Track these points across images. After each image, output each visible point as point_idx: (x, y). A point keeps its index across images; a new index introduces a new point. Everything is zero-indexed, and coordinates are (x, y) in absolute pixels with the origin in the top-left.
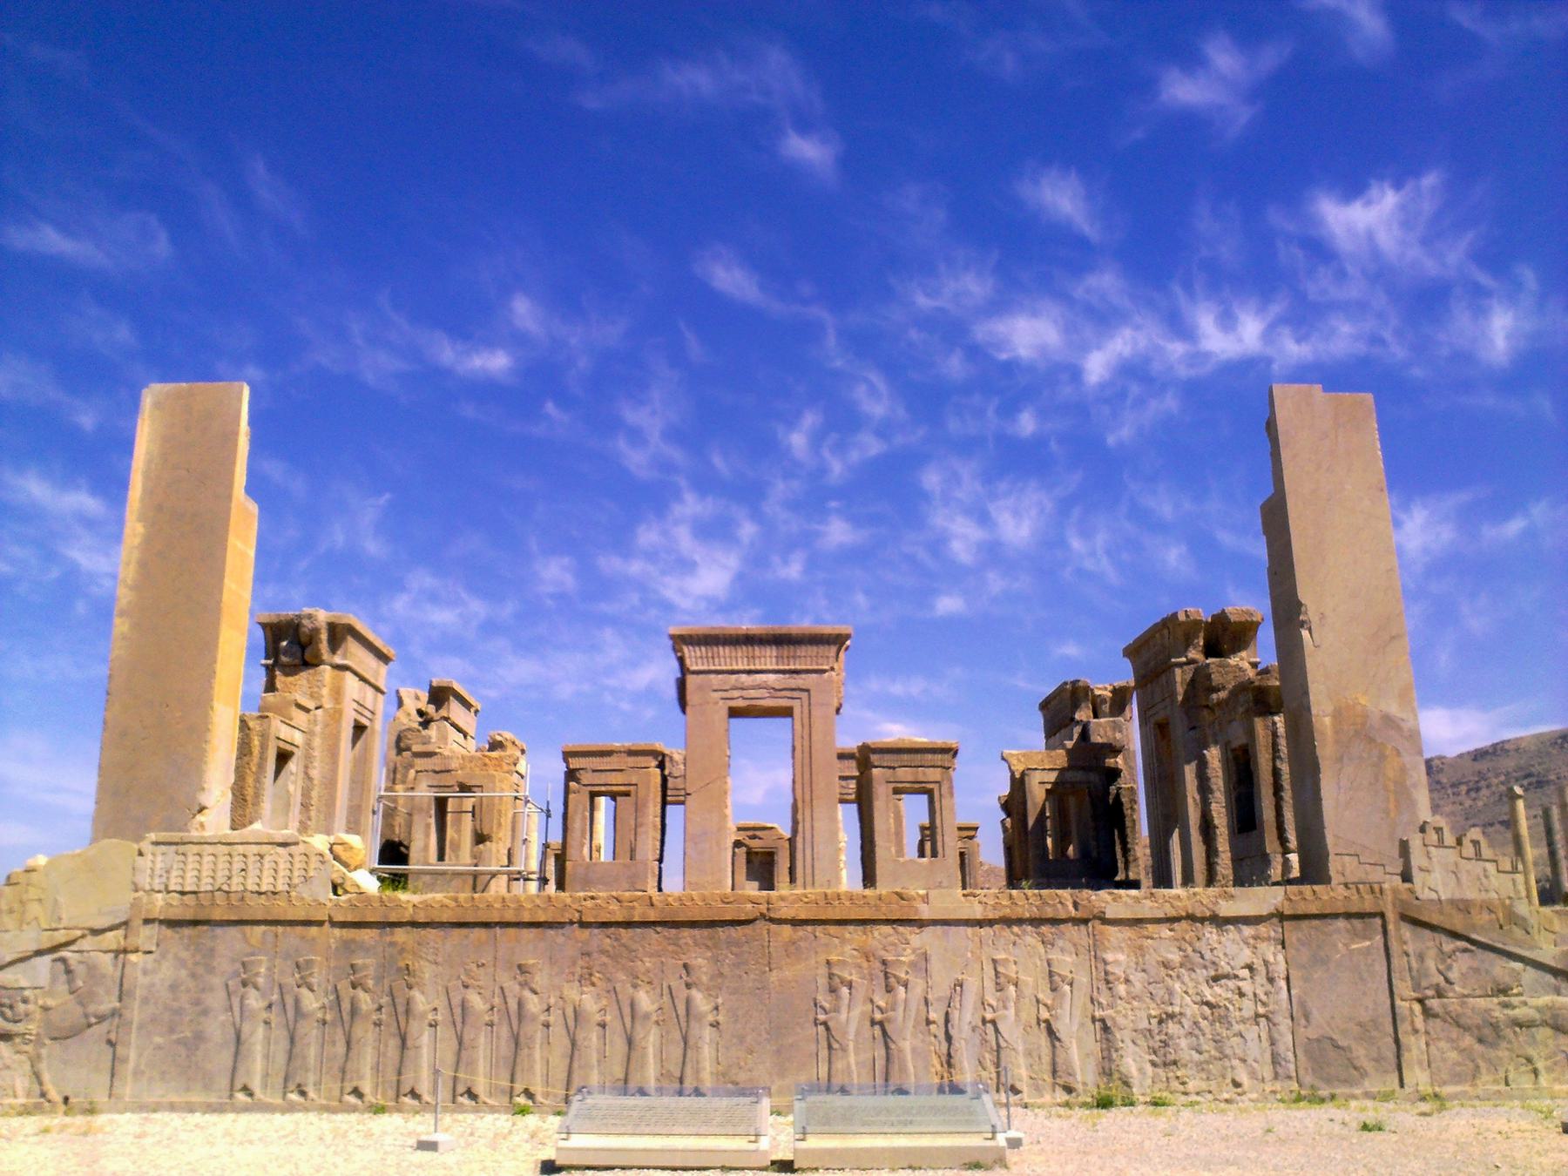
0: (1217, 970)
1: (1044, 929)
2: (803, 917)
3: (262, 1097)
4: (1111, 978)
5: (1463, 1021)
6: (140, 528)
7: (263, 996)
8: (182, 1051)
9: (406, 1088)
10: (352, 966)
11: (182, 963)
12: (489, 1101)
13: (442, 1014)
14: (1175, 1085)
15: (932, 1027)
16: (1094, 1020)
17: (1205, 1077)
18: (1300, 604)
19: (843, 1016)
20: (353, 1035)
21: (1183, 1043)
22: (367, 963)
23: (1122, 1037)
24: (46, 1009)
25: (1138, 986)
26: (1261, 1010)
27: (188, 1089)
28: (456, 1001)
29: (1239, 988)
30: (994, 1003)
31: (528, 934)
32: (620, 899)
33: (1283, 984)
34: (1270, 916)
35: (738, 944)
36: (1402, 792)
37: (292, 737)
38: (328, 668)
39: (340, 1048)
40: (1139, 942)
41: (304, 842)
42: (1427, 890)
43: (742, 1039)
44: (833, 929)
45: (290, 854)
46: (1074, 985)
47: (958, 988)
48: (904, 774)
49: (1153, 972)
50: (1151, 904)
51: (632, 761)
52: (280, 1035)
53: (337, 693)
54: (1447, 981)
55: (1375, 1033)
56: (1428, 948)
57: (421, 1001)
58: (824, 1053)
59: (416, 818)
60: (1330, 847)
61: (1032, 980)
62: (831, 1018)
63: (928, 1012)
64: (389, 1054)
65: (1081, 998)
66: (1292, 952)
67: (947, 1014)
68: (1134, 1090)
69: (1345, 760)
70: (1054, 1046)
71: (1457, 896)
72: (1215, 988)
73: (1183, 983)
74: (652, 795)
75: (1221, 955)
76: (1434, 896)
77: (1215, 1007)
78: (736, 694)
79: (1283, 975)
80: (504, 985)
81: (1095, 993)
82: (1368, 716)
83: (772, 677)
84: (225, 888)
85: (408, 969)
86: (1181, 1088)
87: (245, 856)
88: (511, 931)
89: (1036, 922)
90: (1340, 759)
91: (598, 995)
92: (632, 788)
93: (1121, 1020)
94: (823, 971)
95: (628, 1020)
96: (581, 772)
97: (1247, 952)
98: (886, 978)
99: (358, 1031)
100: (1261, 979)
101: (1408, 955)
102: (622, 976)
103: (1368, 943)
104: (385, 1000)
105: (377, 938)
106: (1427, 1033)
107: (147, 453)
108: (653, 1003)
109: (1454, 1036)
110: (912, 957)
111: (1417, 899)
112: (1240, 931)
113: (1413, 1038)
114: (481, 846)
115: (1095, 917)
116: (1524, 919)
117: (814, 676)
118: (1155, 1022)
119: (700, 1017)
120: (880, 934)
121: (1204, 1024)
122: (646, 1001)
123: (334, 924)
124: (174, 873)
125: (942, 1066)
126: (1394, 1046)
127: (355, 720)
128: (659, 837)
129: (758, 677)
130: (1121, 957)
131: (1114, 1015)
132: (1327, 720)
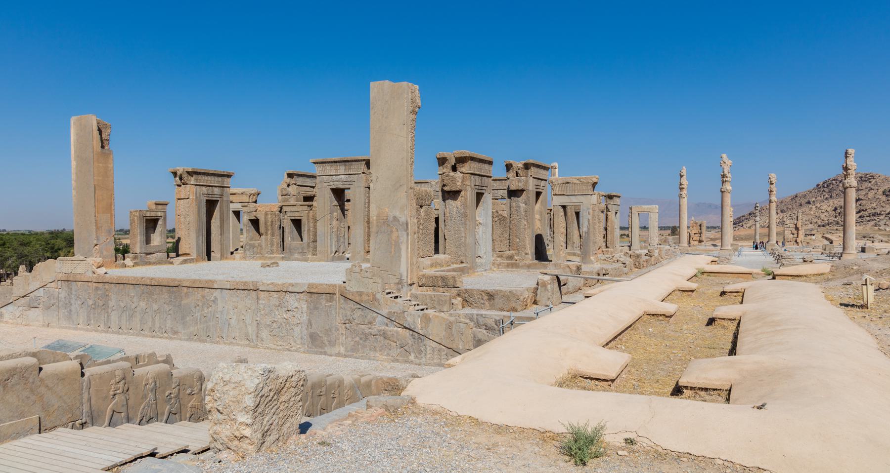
15: (217, 319)
19: (196, 315)
24: (43, 302)
26: (298, 322)
36: (397, 245)
55: (330, 333)
69: (379, 233)
76: (351, 289)
78: (332, 183)
82: (388, 217)
90: (377, 233)
97: (296, 304)
103: (330, 304)
106: (345, 334)
116: (378, 300)
117: (357, 175)
121: (284, 324)
132: (375, 218)
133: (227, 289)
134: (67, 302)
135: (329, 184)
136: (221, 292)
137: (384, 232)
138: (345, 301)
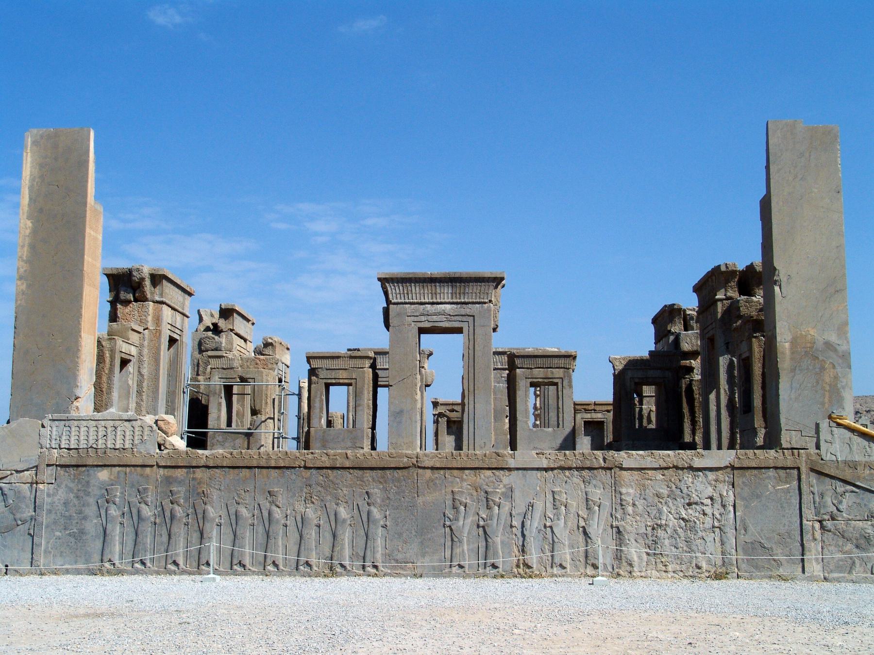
0: (690, 500)
1: (585, 473)
2: (438, 465)
3: (120, 566)
4: (624, 503)
5: (846, 535)
6: (29, 224)
7: (119, 508)
8: (73, 540)
10: (171, 491)
11: (71, 490)
12: (251, 568)
13: (224, 519)
14: (660, 566)
15: (514, 529)
16: (612, 527)
17: (679, 563)
18: (775, 269)
19: (461, 523)
20: (172, 531)
21: (667, 542)
22: (180, 491)
23: (630, 538)
25: (640, 507)
26: (716, 524)
27: (76, 562)
28: (232, 511)
29: (703, 511)
30: (552, 517)
31: (274, 473)
32: (328, 454)
33: (731, 509)
34: (726, 467)
35: (399, 480)
37: (130, 352)
38: (151, 303)
39: (165, 538)
40: (643, 482)
41: (141, 419)
42: (829, 454)
43: (400, 535)
44: (455, 472)
45: (132, 427)
46: (601, 507)
47: (530, 508)
48: (539, 373)
49: (650, 500)
50: (652, 459)
51: (352, 363)
52: (130, 530)
54: (838, 510)
56: (827, 490)
57: (211, 511)
58: (448, 543)
59: (211, 399)
60: (782, 425)
61: (576, 504)
62: (453, 524)
63: (512, 521)
64: (193, 542)
65: (606, 512)
66: (738, 490)
67: (523, 523)
68: (635, 569)
69: (798, 371)
70: (587, 542)
71: (849, 458)
72: (689, 510)
73: (668, 506)
74: (366, 386)
75: (693, 491)
76: (834, 458)
77: (687, 521)
78: (423, 318)
79: (732, 503)
80: (260, 503)
81: (614, 512)
83: (448, 306)
84: (94, 446)
85: (204, 493)
86: (664, 568)
87: (105, 427)
88: (264, 471)
89: (580, 469)
90: (793, 370)
91: (316, 509)
92: (353, 381)
93: (628, 528)
94: (450, 497)
95: (333, 523)
96: (319, 370)
97: (710, 489)
98: (487, 501)
99: (175, 529)
100: (718, 505)
101: (813, 494)
102: (329, 498)
104: (191, 511)
105: (185, 475)
107: (31, 175)
108: (348, 514)
109: (841, 544)
110: (503, 490)
111: (822, 459)
112: (706, 476)
113: (813, 544)
114: (255, 417)
115: (616, 467)
118: (649, 529)
119: (376, 522)
120: (485, 476)
121: (680, 531)
122: (343, 513)
123: (159, 466)
124: (64, 438)
125: (519, 552)
126: (800, 548)
127: (170, 336)
128: (371, 413)
129: (440, 305)
130: (631, 491)
131: (624, 524)
132: (787, 345)
133: (538, 469)
134: (72, 512)
135: (416, 319)
136: (524, 476)
137: (808, 369)
138: (818, 479)
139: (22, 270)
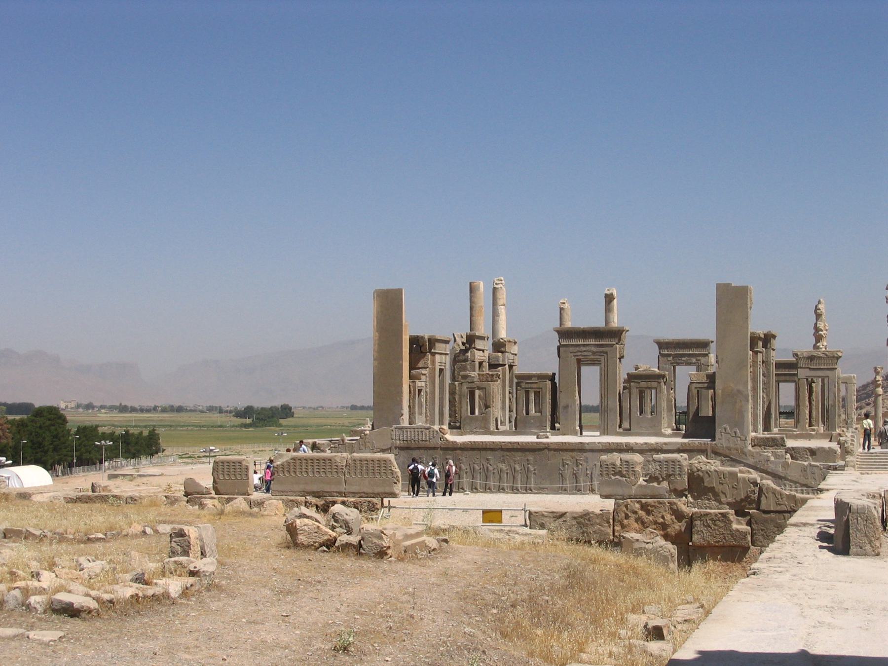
9: (460, 487)
53: (433, 362)
74: (548, 392)
78: (579, 354)
94: (561, 461)
119: (531, 471)
122: (518, 467)
132: (720, 391)
135: (575, 354)
139: (375, 356)
